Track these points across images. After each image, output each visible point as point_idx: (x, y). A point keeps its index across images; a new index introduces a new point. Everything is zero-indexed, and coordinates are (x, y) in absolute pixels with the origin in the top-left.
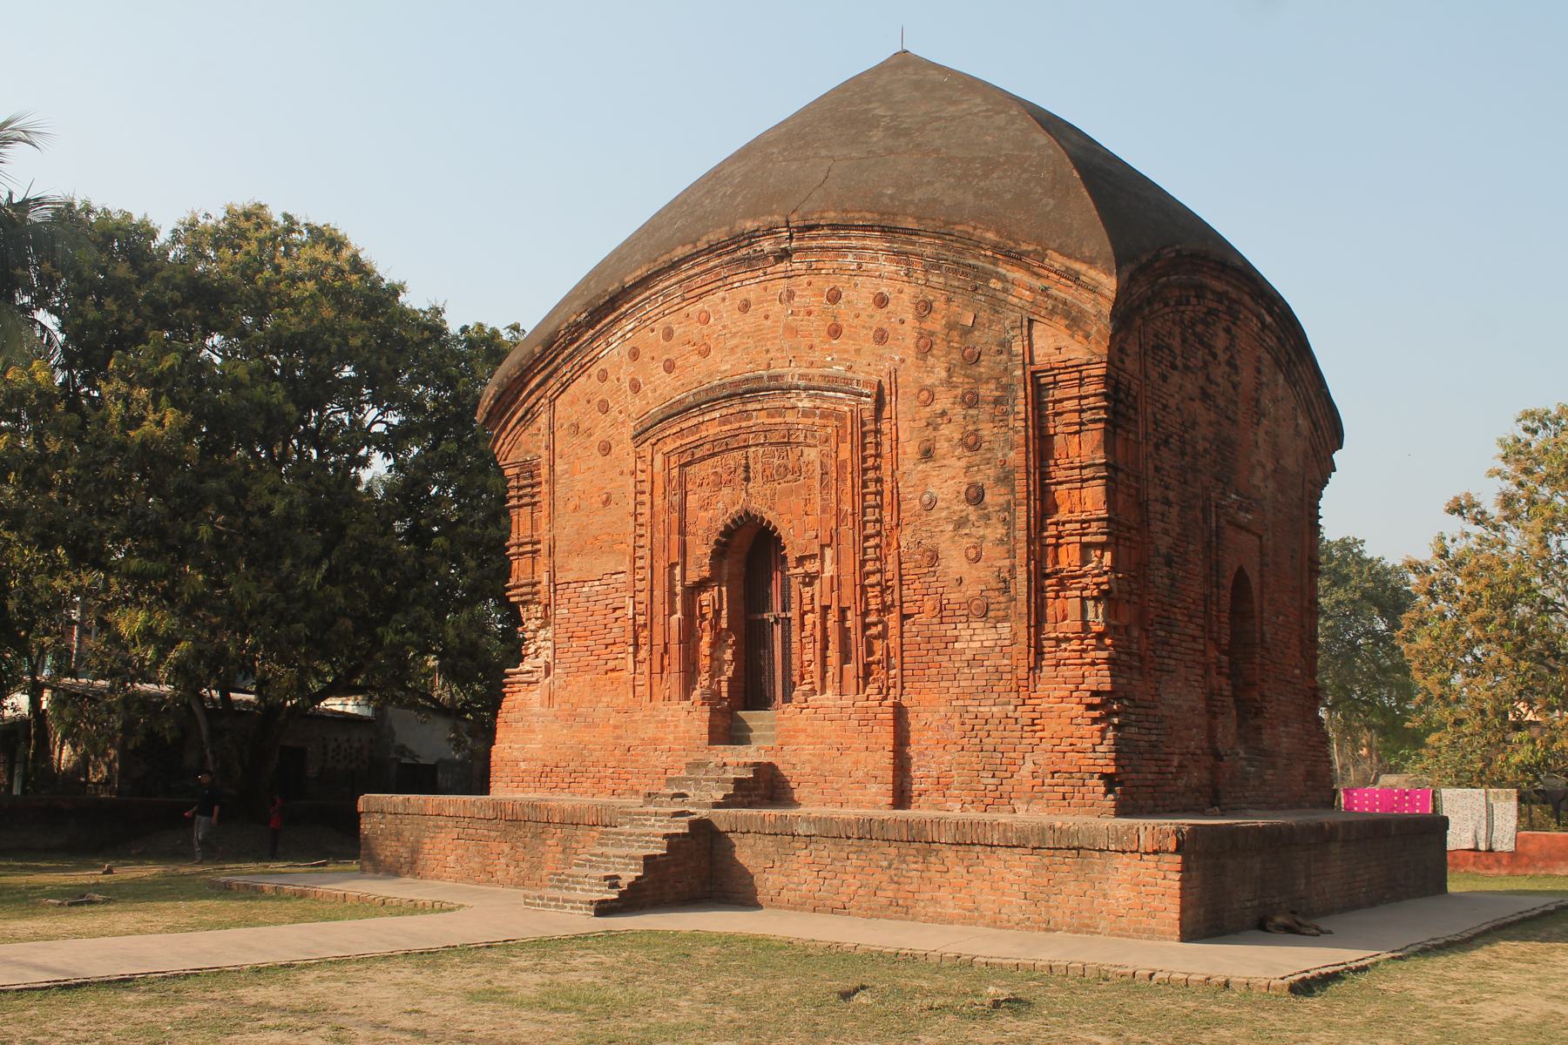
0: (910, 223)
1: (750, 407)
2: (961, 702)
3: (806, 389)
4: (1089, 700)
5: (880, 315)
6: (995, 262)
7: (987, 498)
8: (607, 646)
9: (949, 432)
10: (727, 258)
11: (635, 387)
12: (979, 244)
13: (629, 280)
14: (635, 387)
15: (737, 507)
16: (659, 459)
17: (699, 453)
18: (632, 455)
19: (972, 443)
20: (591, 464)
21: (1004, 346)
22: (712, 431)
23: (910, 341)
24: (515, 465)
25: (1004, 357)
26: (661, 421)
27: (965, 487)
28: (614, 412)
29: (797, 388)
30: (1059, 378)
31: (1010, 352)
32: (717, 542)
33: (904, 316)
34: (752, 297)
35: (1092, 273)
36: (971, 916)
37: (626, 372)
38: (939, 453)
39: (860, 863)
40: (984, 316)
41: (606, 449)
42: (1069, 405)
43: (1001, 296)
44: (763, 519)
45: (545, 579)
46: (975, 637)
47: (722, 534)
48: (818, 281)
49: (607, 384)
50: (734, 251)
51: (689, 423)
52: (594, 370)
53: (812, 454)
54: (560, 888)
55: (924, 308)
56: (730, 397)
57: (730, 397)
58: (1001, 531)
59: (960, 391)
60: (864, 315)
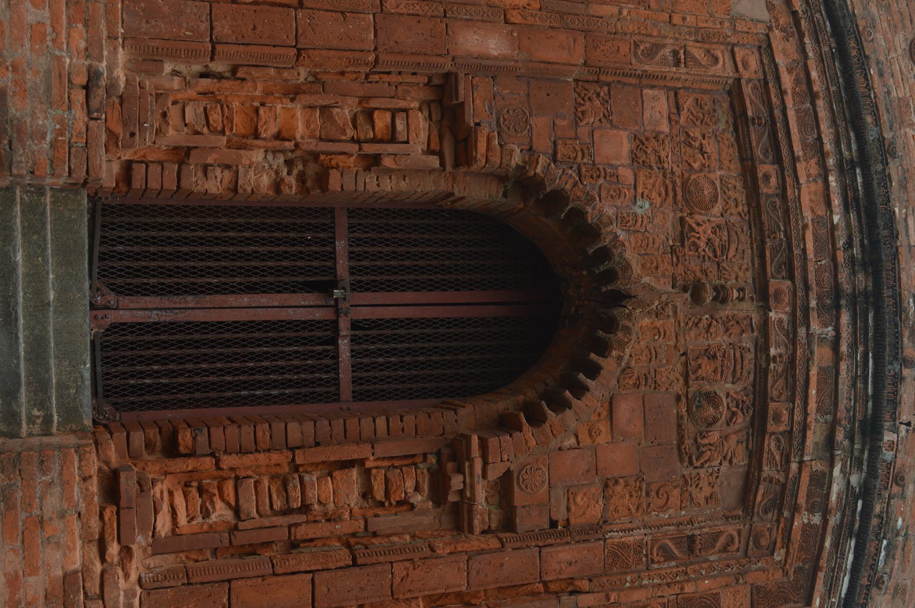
1: (845, 318)
17: (758, 142)
26: (838, 34)
29: (872, 472)
44: (603, 349)
47: (578, 213)
51: (823, 114)
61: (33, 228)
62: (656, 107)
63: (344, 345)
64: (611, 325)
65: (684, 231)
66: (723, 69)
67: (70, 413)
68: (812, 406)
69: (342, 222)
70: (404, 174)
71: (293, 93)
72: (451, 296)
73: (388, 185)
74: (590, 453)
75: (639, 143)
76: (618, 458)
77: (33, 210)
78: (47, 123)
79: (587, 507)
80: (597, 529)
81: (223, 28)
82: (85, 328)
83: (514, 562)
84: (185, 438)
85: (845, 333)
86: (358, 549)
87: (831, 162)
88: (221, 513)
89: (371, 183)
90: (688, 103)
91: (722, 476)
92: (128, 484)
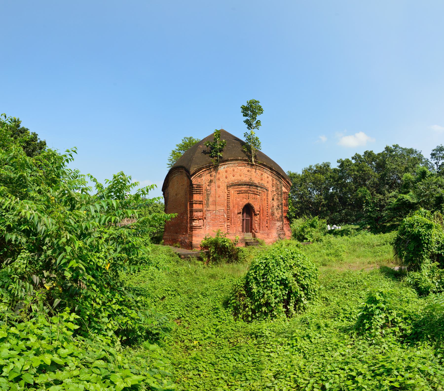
0: (274, 169)
9: (275, 198)
11: (226, 178)
12: (281, 175)
13: (229, 159)
14: (226, 178)
16: (233, 192)
19: (278, 199)
21: (281, 188)
24: (196, 185)
28: (221, 180)
37: (225, 174)
41: (219, 187)
53: (258, 196)
55: (273, 181)
56: (248, 185)
57: (248, 185)
83: (261, 211)
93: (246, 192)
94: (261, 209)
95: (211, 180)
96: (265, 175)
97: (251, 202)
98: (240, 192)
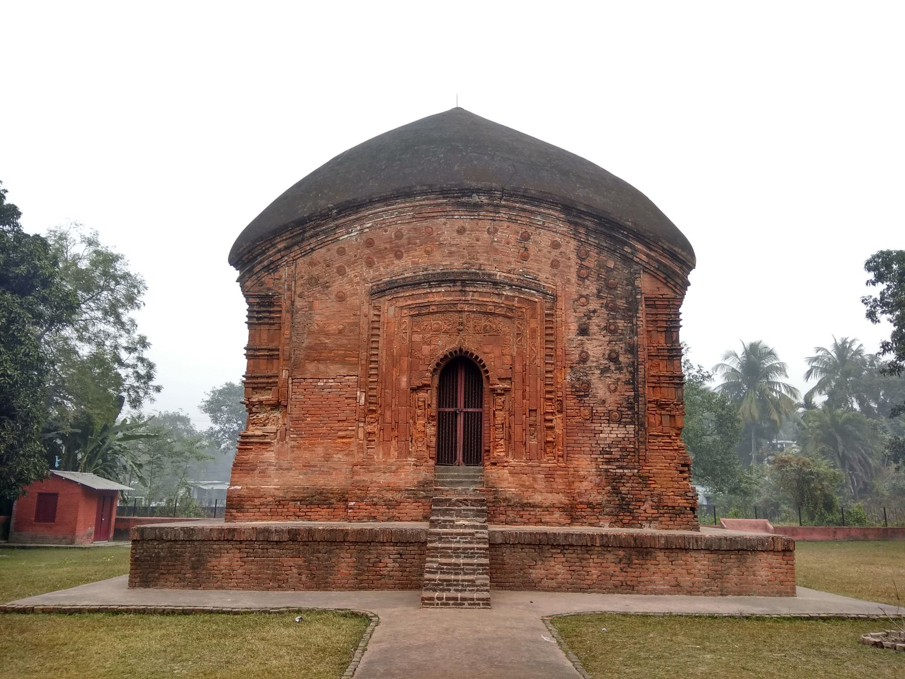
1: (467, 289)
2: (605, 467)
3: (511, 285)
4: (681, 468)
5: (555, 253)
6: (627, 237)
7: (621, 359)
8: (339, 421)
10: (453, 200)
15: (454, 345)
17: (425, 311)
18: (366, 305)
19: (610, 329)
20: (329, 305)
21: (631, 282)
22: (437, 299)
23: (574, 270)
25: (630, 287)
26: (397, 287)
27: (608, 352)
29: (506, 284)
30: (657, 303)
31: (633, 285)
32: (438, 365)
33: (571, 256)
34: (467, 226)
35: (684, 254)
36: (677, 588)
38: (591, 331)
39: (599, 561)
40: (620, 265)
42: (660, 317)
43: (631, 256)
44: (472, 354)
45: (285, 374)
46: (611, 433)
47: (441, 360)
48: (515, 227)
49: (345, 258)
50: (459, 197)
52: (335, 247)
54: (435, 590)
58: (628, 376)
59: (605, 301)
60: (545, 251)
61: (442, 477)
62: (417, 338)
63: (470, 410)
64: (467, 352)
65: (446, 332)
66: (407, 320)
67: (480, 471)
68: (488, 300)
69: (441, 409)
70: (432, 398)
71: (415, 423)
72: (459, 383)
73: (434, 402)
74: (494, 360)
75: (425, 343)
76: (497, 352)
77: (439, 477)
78: (424, 474)
79: (507, 360)
80: (513, 358)
81: (403, 439)
82: (463, 467)
83: (517, 379)
84: (487, 448)
85: (472, 289)
86: (511, 414)
87: (429, 290)
88: (502, 442)
89: (434, 406)
90: (415, 329)
91: (502, 325)
92: (493, 461)
93: (444, 310)
94: (518, 367)
95: (311, 278)
96: (543, 239)
97: (471, 345)
98: (420, 312)
